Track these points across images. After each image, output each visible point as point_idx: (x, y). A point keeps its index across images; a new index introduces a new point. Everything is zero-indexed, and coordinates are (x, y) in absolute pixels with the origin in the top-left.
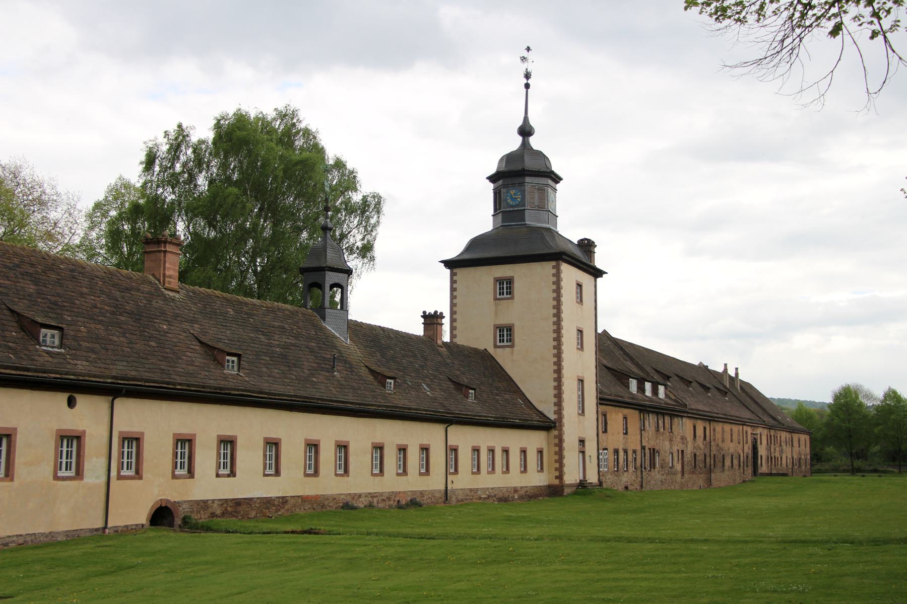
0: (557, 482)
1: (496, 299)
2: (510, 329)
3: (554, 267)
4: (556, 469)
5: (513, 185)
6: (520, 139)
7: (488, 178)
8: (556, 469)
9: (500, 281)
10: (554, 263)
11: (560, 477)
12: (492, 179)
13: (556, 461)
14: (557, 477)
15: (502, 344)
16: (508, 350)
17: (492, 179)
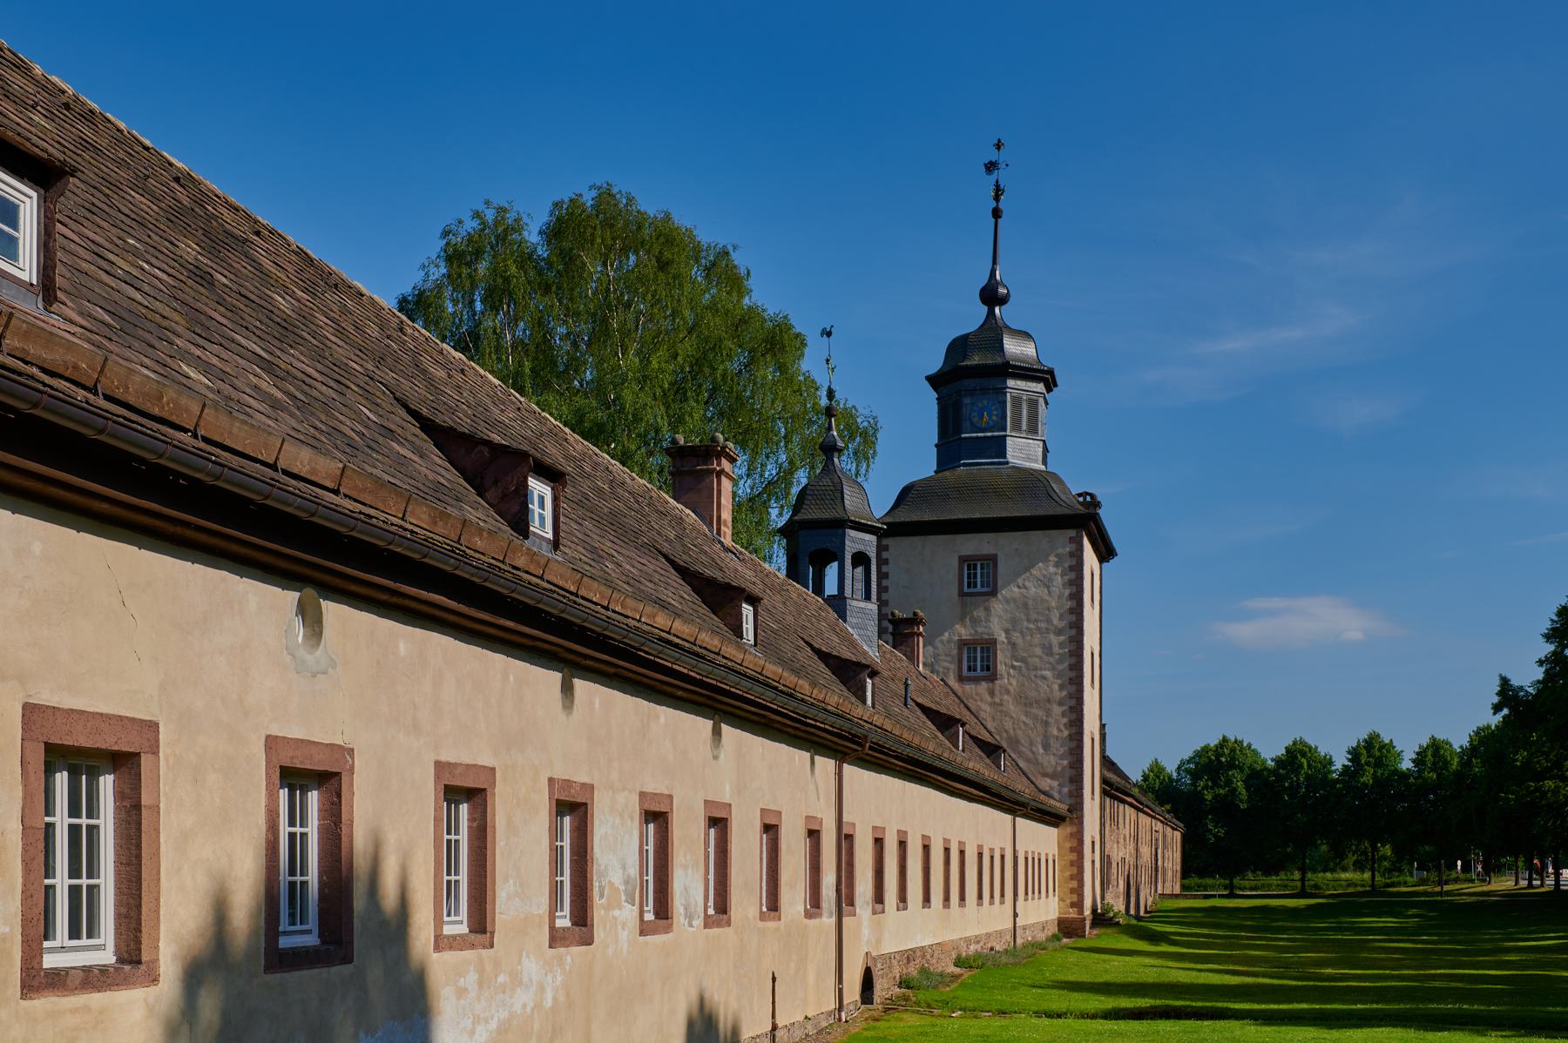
0: (1073, 914)
1: (962, 594)
2: (989, 646)
3: (1071, 540)
4: (1072, 891)
5: (984, 390)
6: (983, 310)
7: (929, 378)
8: (1072, 891)
9: (969, 562)
10: (1072, 533)
11: (1078, 905)
12: (934, 381)
13: (1072, 878)
14: (1073, 905)
15: (972, 674)
16: (983, 686)
17: (934, 381)
